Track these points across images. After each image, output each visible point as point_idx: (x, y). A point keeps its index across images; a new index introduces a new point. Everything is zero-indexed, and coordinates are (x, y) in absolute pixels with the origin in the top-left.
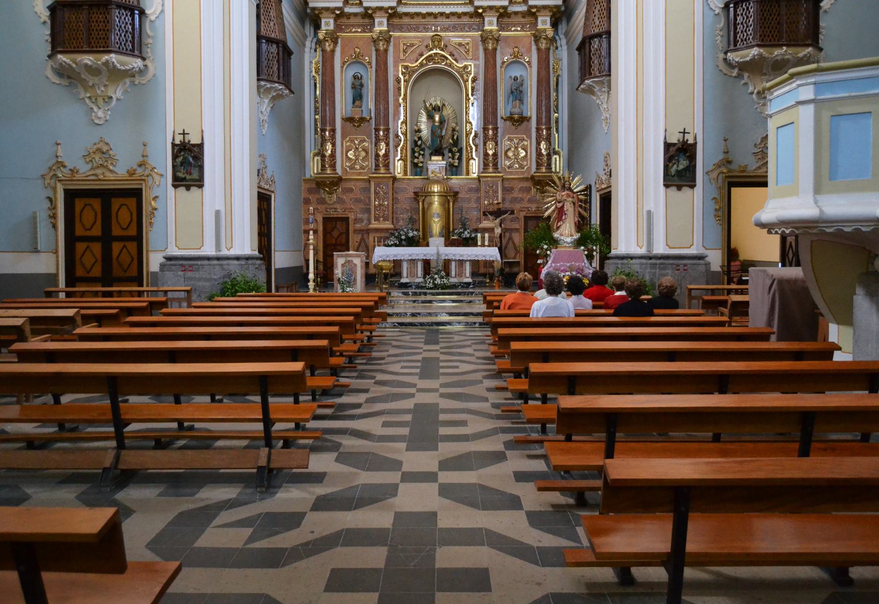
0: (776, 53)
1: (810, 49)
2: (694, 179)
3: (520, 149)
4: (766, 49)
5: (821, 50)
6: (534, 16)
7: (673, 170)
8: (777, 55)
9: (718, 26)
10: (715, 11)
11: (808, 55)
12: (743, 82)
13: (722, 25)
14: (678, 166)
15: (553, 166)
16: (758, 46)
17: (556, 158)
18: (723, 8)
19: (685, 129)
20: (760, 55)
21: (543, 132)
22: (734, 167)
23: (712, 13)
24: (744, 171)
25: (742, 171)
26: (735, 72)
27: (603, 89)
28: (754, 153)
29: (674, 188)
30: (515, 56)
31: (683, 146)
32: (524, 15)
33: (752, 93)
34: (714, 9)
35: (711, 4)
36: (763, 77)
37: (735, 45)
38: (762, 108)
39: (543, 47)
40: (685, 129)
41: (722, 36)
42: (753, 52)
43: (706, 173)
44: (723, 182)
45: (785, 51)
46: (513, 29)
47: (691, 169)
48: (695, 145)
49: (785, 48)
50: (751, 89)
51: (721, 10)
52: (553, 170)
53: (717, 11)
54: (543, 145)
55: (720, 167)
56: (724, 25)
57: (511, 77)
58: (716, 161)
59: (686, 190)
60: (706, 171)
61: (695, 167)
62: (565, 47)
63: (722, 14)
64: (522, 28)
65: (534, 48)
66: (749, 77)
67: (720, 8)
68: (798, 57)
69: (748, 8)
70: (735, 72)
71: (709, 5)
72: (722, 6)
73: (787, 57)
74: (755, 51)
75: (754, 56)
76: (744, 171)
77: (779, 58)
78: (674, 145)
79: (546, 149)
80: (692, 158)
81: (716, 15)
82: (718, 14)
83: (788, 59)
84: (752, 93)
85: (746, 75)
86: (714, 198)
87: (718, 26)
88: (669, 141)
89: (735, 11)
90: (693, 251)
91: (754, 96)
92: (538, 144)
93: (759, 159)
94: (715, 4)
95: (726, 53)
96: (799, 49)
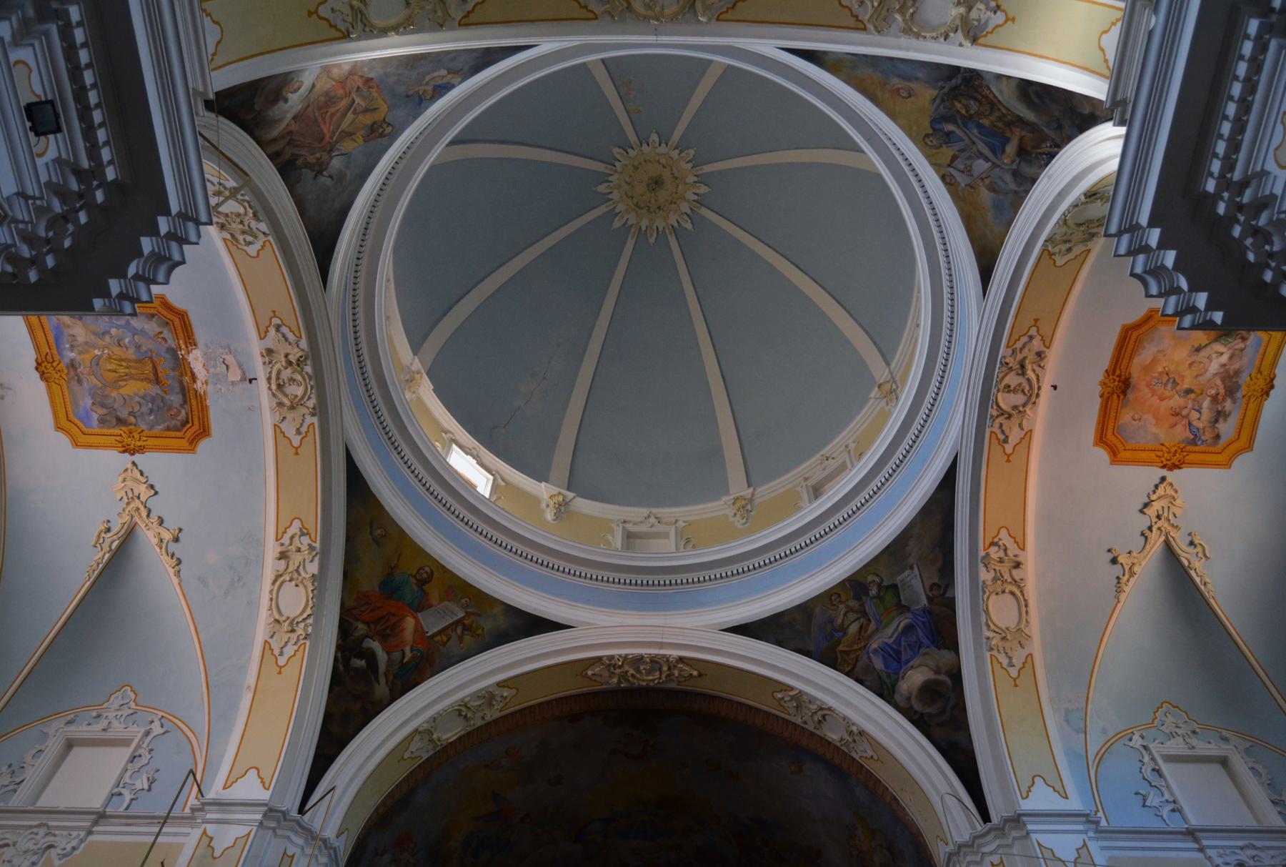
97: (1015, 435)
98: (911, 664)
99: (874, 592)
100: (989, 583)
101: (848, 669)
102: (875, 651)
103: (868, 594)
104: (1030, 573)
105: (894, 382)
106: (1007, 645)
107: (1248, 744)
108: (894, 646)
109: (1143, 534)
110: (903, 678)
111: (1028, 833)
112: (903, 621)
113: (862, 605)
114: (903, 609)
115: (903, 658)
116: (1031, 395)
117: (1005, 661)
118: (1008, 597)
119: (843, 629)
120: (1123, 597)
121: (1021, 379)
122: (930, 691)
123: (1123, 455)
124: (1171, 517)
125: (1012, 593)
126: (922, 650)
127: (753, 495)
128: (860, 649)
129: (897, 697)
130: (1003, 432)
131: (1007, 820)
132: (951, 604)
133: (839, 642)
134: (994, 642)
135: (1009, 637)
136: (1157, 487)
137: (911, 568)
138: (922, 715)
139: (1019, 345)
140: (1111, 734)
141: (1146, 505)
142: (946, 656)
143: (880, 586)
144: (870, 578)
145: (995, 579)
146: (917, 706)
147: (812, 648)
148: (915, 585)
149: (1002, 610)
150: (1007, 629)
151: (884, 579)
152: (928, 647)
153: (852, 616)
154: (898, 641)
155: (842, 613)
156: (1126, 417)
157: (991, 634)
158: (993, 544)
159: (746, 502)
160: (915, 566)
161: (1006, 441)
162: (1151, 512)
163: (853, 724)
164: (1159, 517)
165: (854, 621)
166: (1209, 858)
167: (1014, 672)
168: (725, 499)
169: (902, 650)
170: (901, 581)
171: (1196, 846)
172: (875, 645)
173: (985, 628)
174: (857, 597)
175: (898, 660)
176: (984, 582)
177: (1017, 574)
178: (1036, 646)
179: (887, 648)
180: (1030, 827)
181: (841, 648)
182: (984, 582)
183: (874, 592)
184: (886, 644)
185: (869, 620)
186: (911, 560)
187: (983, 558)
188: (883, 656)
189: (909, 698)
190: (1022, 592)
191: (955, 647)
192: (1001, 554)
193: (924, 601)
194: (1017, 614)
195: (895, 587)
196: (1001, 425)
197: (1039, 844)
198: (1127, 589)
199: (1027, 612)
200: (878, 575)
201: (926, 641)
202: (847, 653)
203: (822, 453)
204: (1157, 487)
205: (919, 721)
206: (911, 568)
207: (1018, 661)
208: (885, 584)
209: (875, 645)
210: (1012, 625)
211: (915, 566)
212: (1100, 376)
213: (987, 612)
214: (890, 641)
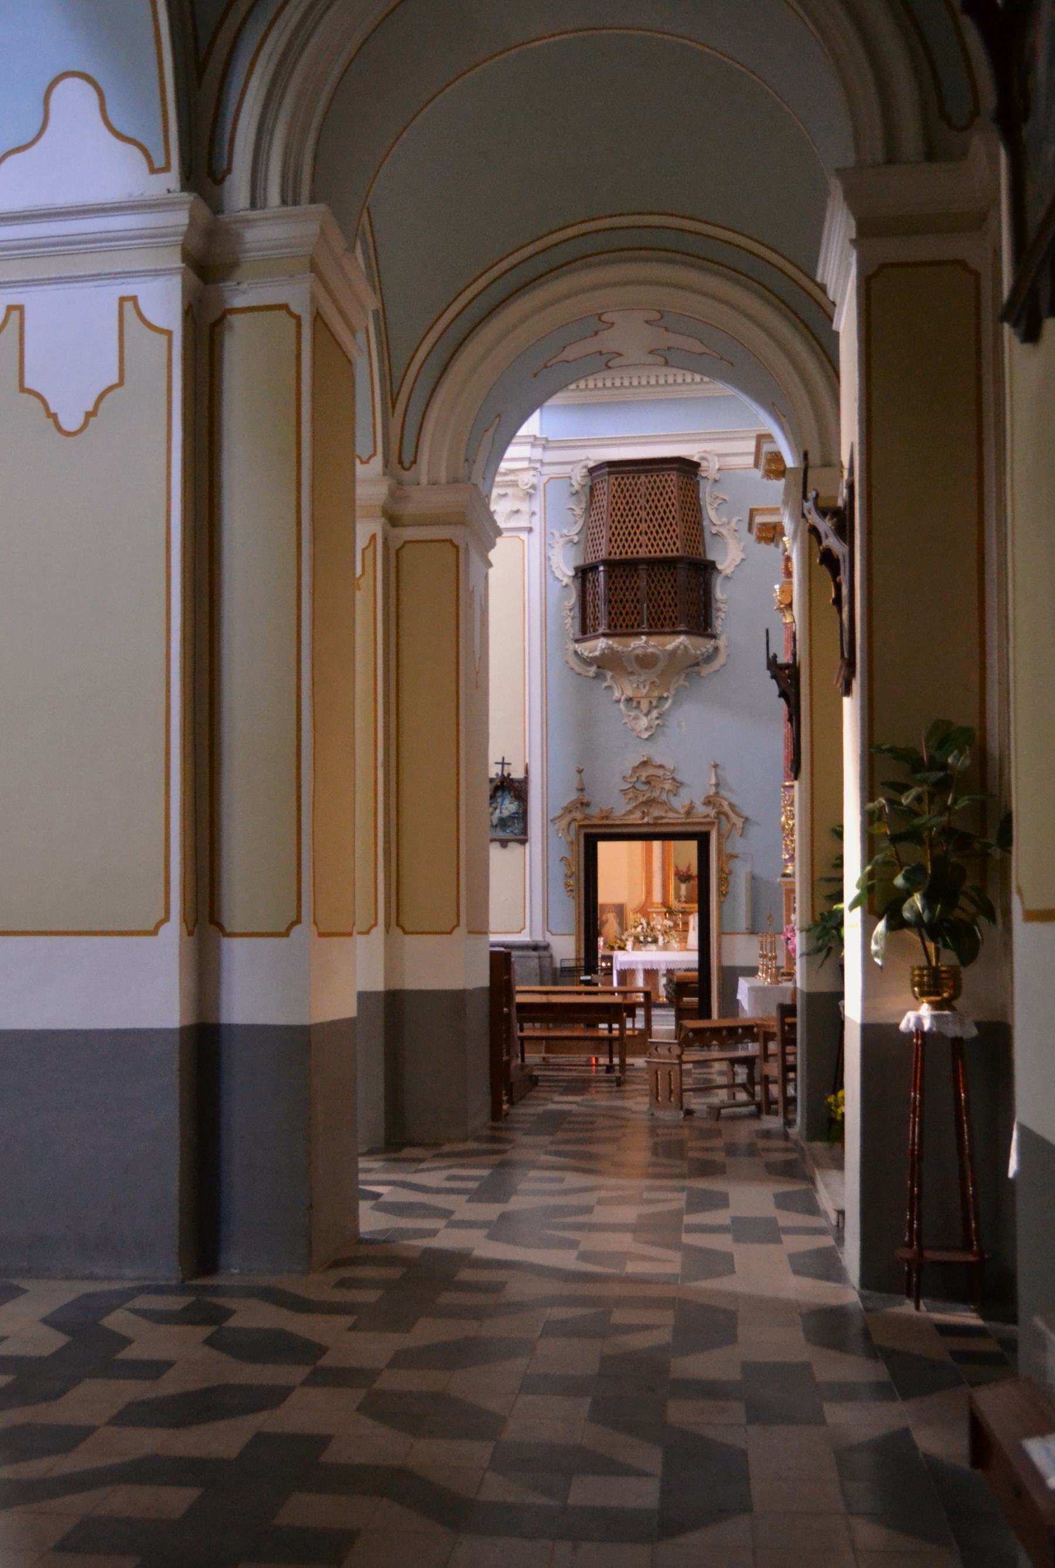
0: (632, 645)
2: (525, 831)
4: (617, 639)
8: (634, 649)
9: (566, 603)
10: (562, 581)
11: (682, 647)
12: (605, 684)
16: (605, 635)
19: (503, 758)
22: (593, 811)
23: (559, 585)
24: (607, 818)
25: (603, 818)
26: (592, 670)
28: (622, 791)
31: (502, 783)
33: (618, 701)
34: (561, 578)
36: (631, 678)
38: (634, 722)
40: (503, 758)
41: (573, 618)
43: (552, 820)
44: (577, 835)
45: (646, 642)
47: (522, 815)
48: (525, 781)
49: (644, 638)
50: (617, 694)
51: (571, 579)
55: (570, 811)
56: (575, 602)
58: (565, 804)
60: (551, 817)
63: (572, 586)
66: (612, 677)
67: (570, 576)
68: (666, 650)
71: (553, 572)
72: (572, 573)
73: (650, 650)
74: (602, 643)
75: (603, 650)
76: (607, 818)
77: (639, 652)
82: (566, 586)
83: (653, 654)
84: (618, 701)
85: (609, 674)
87: (566, 603)
90: (524, 938)
91: (622, 706)
93: (630, 799)
94: (562, 571)
96: (667, 638)
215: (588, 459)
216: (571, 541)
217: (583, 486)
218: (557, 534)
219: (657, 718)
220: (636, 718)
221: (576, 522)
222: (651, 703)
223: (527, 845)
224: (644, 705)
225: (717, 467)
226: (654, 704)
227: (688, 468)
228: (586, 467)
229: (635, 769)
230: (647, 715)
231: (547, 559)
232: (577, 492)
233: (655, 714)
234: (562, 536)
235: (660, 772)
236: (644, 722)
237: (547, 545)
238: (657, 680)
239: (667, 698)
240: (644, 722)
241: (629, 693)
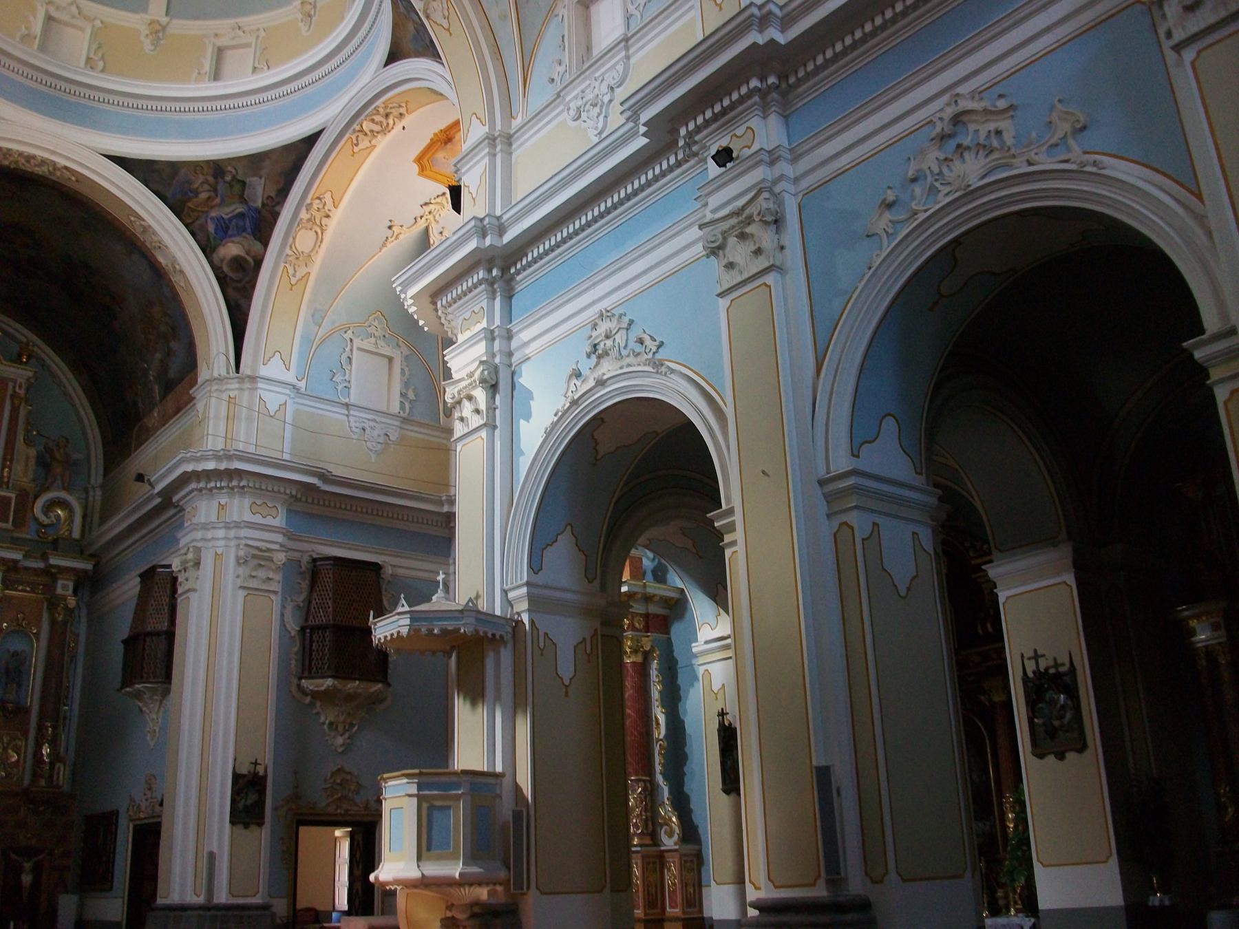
1: (380, 685)
3: (10, 751)
4: (340, 680)
5: (389, 685)
6: (54, 578)
7: (241, 805)
13: (296, 649)
14: (246, 801)
15: (55, 778)
17: (59, 769)
18: (299, 631)
20: (334, 686)
21: (47, 730)
27: (155, 697)
29: (241, 826)
30: (18, 625)
32: (36, 571)
35: (287, 626)
37: (310, 672)
39: (60, 619)
41: (296, 660)
42: (327, 683)
46: (20, 588)
47: (260, 804)
48: (265, 777)
49: (357, 682)
50: (323, 719)
52: (55, 783)
53: (293, 633)
54: (46, 750)
57: (8, 651)
59: (254, 828)
61: (264, 802)
62: (84, 620)
63: (297, 636)
64: (32, 588)
65: (45, 616)
69: (324, 636)
70: (308, 700)
72: (298, 629)
74: (329, 682)
75: (329, 686)
77: (351, 691)
78: (244, 776)
79: (49, 755)
80: (262, 792)
81: (291, 637)
82: (294, 637)
84: (324, 723)
86: (282, 839)
88: (238, 771)
89: (311, 636)
92: (39, 747)
95: (300, 679)
96: (370, 684)
97: (364, 143)
98: (233, 239)
99: (228, 178)
100: (304, 221)
101: (189, 221)
102: (212, 218)
103: (223, 178)
104: (332, 225)
105: (315, 7)
106: (297, 262)
107: (408, 353)
108: (227, 222)
109: (415, 219)
110: (224, 245)
111: (257, 388)
112: (241, 209)
113: (217, 183)
114: (243, 200)
115: (230, 232)
116: (385, 130)
117: (291, 271)
118: (312, 233)
119: (197, 193)
120: (384, 250)
121: (384, 121)
122: (238, 263)
123: (428, 172)
124: (437, 216)
125: (316, 232)
126: (244, 234)
127: (168, 23)
128: (203, 212)
129: (215, 256)
130: (357, 140)
131: (249, 377)
132: (275, 216)
133: (189, 200)
134: (290, 259)
135: (301, 259)
136: (438, 196)
137: (261, 178)
138: (226, 276)
139: (391, 105)
140: (336, 325)
141: (426, 204)
142: (258, 246)
143: (234, 178)
144: (229, 168)
145: (309, 220)
146: (225, 269)
147: (169, 195)
148: (259, 190)
149: (304, 240)
150: (302, 252)
151: (240, 172)
152: (249, 234)
153: (206, 187)
154: (230, 220)
155: (200, 181)
156: (440, 155)
157: (290, 253)
158: (318, 198)
159: (160, 28)
160: (263, 179)
161: (357, 145)
162: (427, 209)
163: (178, 264)
164: (430, 213)
165: (205, 191)
166: (349, 421)
167: (294, 281)
168: (143, 15)
169: (231, 227)
170: (250, 181)
171: (346, 412)
172: (213, 214)
173: (288, 247)
174: (215, 177)
175: (226, 233)
176: (301, 220)
177: (325, 221)
178: (315, 270)
179: (222, 222)
180: (260, 385)
181: (190, 204)
182: (301, 220)
183: (228, 178)
184: (223, 218)
185: (217, 196)
186: (263, 172)
187: (308, 204)
188: (217, 225)
189: (222, 261)
190: (322, 234)
191: (266, 244)
192: (321, 206)
193: (259, 204)
194: (313, 243)
195: (244, 183)
196: (358, 136)
197: (260, 397)
198: (389, 246)
199: (319, 246)
200: (235, 169)
201: (249, 230)
202: (193, 210)
203: (238, 20)
204: (438, 196)
205: (222, 280)
206: (261, 178)
207: (299, 275)
208: (239, 178)
209: (213, 214)
210: (307, 251)
211: (263, 179)
212: (436, 130)
213: (294, 239)
214: (225, 217)
215: (313, 551)
216: (299, 607)
217: (308, 569)
218: (289, 599)
219: (349, 738)
220: (335, 737)
221: (301, 593)
222: (345, 727)
223: (263, 827)
224: (340, 728)
225: (390, 572)
226: (347, 728)
227: (376, 568)
228: (311, 556)
229: (333, 774)
230: (342, 735)
231: (282, 615)
232: (304, 572)
233: (347, 735)
234: (292, 601)
235: (349, 777)
236: (340, 740)
237: (283, 607)
238: (352, 712)
239: (354, 726)
240: (340, 740)
241: (331, 718)
